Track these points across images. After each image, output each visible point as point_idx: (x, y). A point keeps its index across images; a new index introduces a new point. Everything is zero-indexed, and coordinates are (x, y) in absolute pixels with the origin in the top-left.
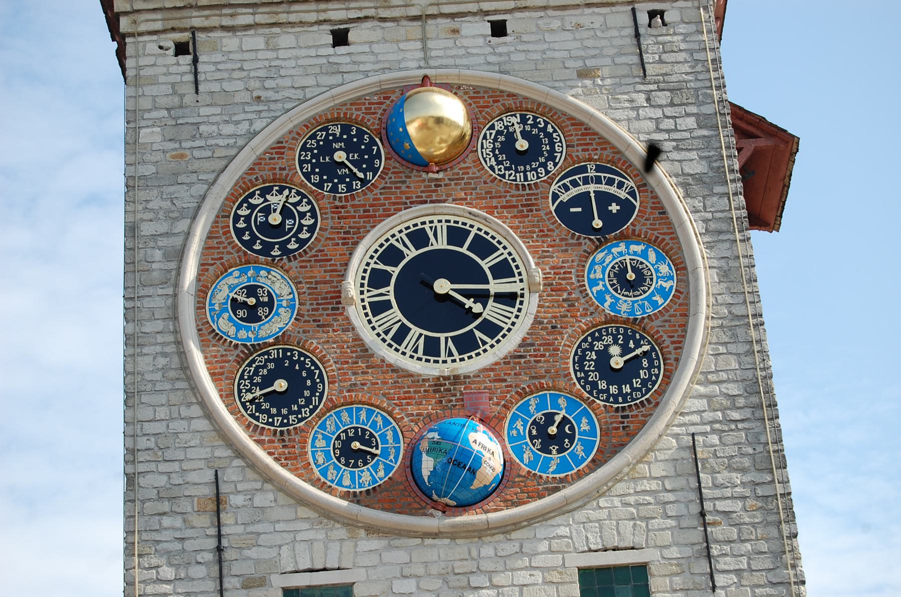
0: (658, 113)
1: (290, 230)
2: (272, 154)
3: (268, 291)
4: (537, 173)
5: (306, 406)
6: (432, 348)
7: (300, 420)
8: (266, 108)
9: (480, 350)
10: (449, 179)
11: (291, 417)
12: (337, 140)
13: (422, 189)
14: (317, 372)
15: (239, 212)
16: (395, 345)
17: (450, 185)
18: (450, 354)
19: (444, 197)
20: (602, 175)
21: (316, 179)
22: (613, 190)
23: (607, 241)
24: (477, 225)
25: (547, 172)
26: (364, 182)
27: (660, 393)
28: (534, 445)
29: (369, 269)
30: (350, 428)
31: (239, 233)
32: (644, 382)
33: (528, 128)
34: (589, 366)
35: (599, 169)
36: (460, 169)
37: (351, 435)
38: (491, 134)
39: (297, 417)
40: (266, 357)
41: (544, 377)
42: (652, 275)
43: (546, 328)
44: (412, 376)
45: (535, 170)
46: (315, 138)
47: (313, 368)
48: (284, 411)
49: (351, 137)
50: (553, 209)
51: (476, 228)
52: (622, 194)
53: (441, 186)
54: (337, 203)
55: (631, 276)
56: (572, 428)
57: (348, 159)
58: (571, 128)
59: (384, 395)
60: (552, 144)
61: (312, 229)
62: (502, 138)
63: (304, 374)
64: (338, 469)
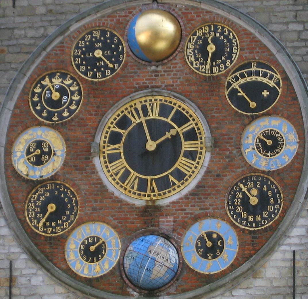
0: (300, 27)
1: (65, 103)
2: (56, 51)
3: (49, 145)
4: (219, 68)
5: (67, 221)
6: (143, 186)
7: (62, 230)
8: (55, 18)
9: (171, 189)
10: (165, 71)
11: (58, 228)
12: (97, 41)
13: (147, 77)
14: (74, 199)
15: (35, 90)
16: (121, 183)
17: (164, 75)
18: (153, 191)
19: (160, 84)
20: (261, 70)
21: (83, 68)
22: (266, 80)
23: (257, 117)
24: (179, 103)
25: (226, 67)
26: (113, 70)
27: (278, 223)
28: (198, 252)
29: (109, 131)
30: (90, 237)
31: (35, 104)
32: (270, 214)
33: (217, 35)
34: (237, 203)
35: (260, 65)
36: (172, 64)
37: (90, 241)
38: (193, 39)
39: (61, 228)
40: (44, 188)
41: (209, 209)
42: (283, 141)
43: (214, 176)
44: (129, 204)
45: (218, 66)
46: (84, 40)
47: (71, 196)
48: (54, 224)
49: (106, 39)
50: (227, 93)
51: (177, 105)
52: (272, 84)
53: (158, 76)
54: (94, 87)
55: (269, 142)
56: (222, 243)
57: (103, 55)
58: (243, 36)
59: (112, 216)
60: (231, 48)
61: (78, 103)
62: (200, 42)
63: (66, 200)
64: (82, 263)
